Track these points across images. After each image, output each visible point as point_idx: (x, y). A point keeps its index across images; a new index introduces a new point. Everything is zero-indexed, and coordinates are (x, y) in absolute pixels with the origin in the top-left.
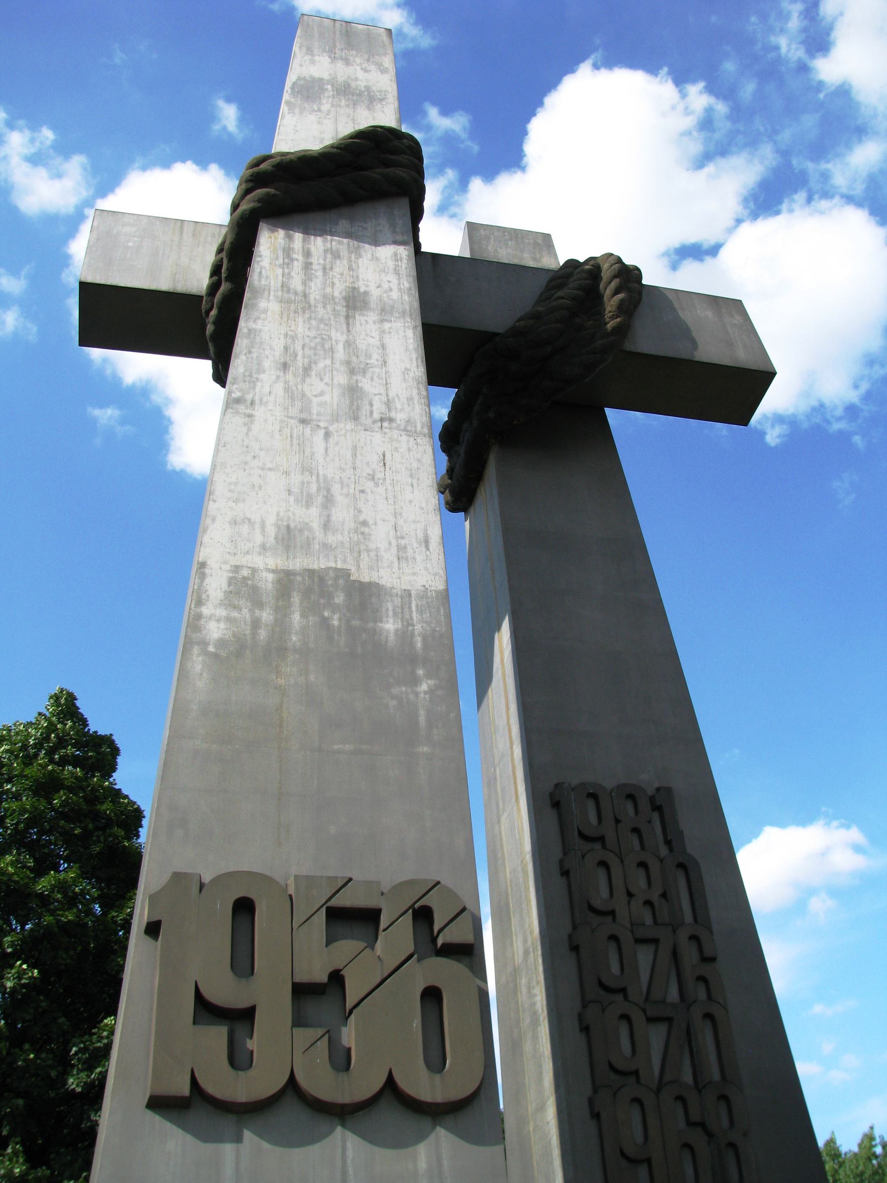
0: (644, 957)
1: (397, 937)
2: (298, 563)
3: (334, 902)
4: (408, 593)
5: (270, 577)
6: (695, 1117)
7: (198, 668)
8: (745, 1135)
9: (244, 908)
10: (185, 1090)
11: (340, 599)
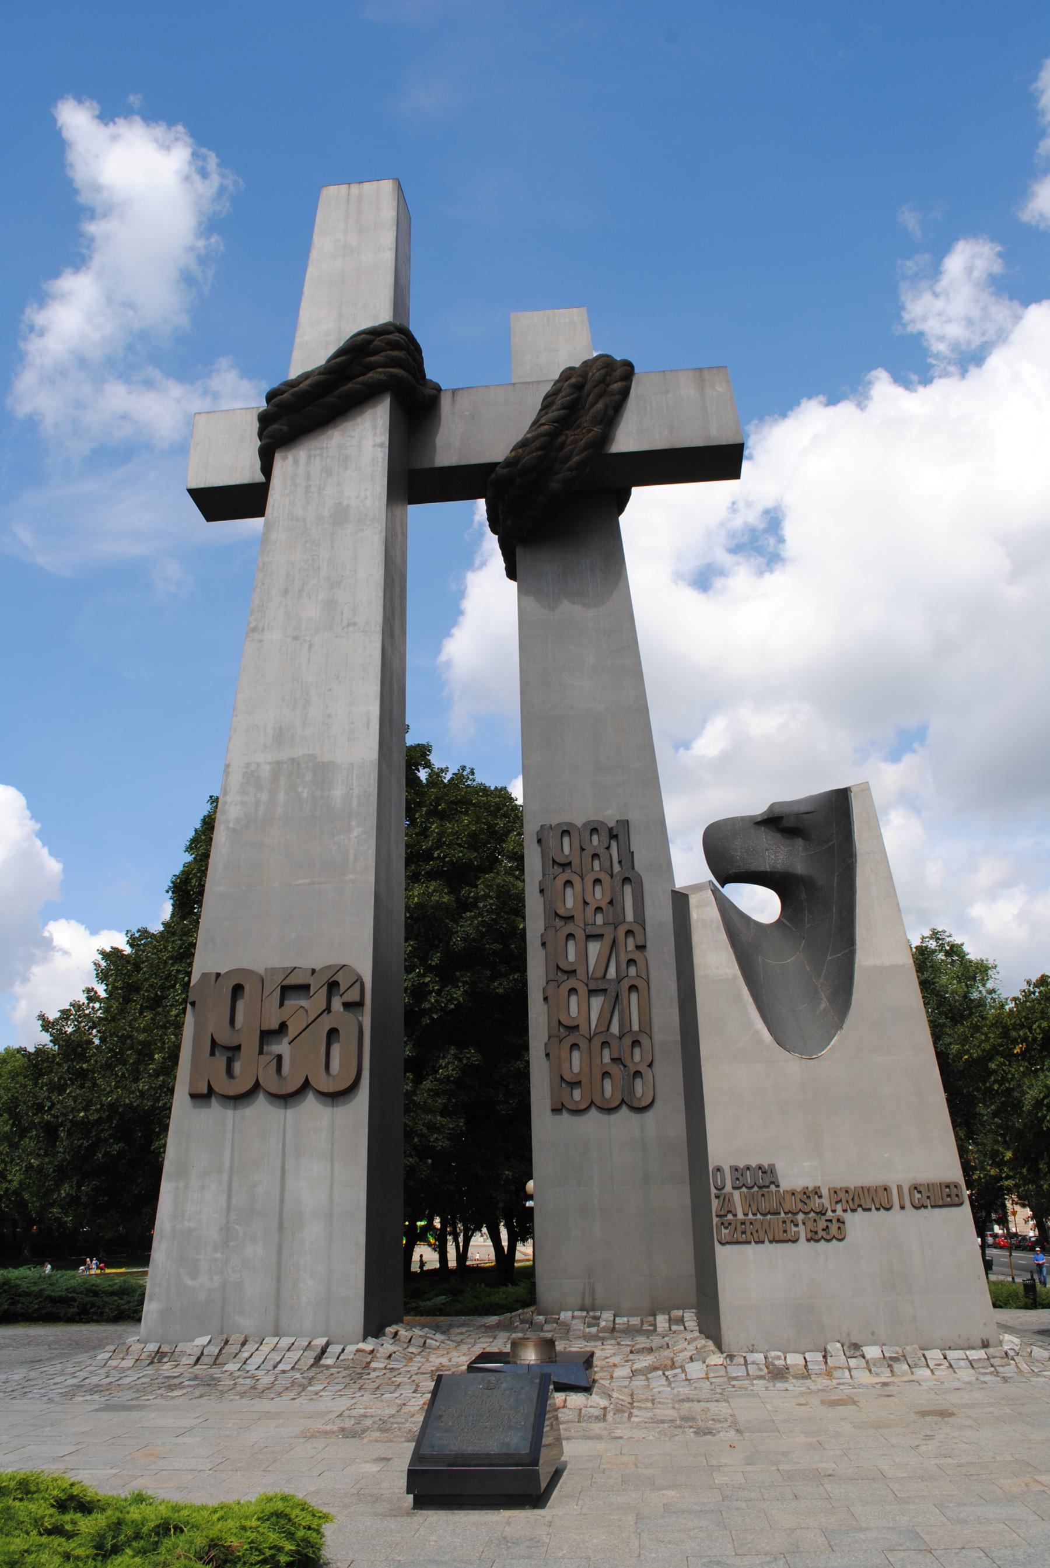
2: (285, 754)
3: (285, 983)
4: (352, 765)
5: (268, 767)
6: (616, 1056)
7: (223, 839)
8: (650, 1065)
9: (238, 990)
10: (205, 1091)
11: (309, 777)
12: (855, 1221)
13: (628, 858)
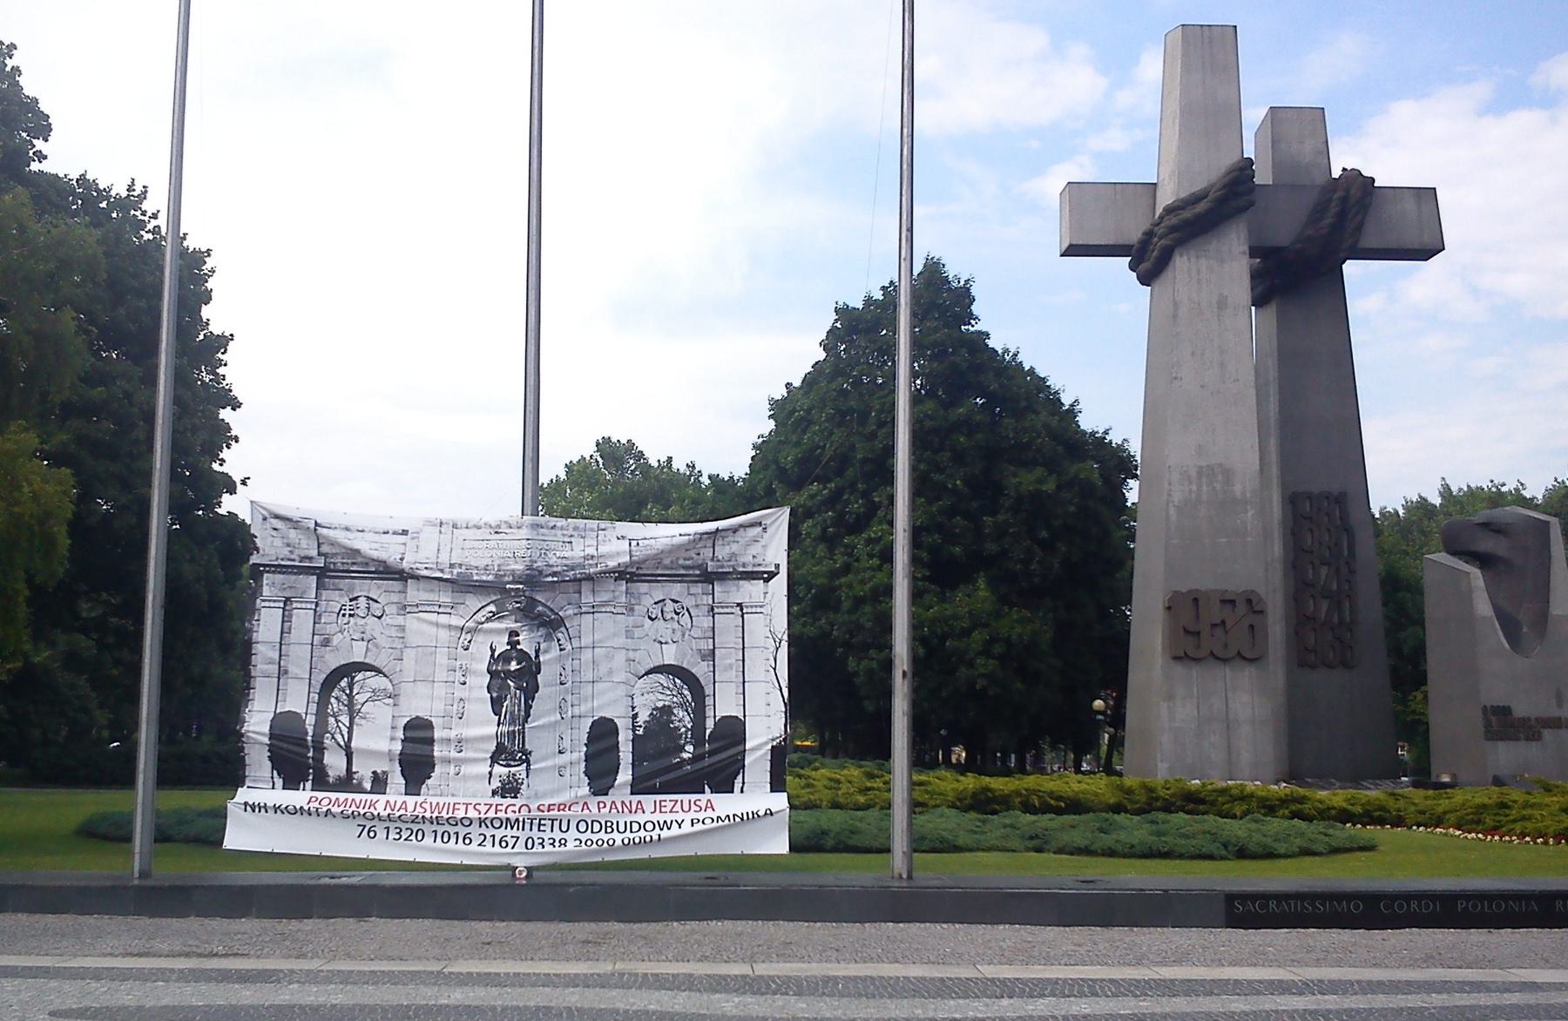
0: (1324, 571)
1: (1241, 608)
2: (1203, 464)
12: (1547, 734)
13: (1344, 516)
